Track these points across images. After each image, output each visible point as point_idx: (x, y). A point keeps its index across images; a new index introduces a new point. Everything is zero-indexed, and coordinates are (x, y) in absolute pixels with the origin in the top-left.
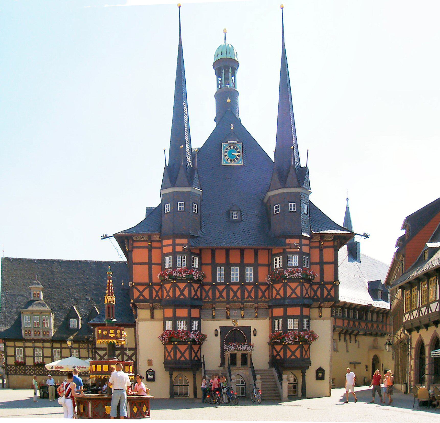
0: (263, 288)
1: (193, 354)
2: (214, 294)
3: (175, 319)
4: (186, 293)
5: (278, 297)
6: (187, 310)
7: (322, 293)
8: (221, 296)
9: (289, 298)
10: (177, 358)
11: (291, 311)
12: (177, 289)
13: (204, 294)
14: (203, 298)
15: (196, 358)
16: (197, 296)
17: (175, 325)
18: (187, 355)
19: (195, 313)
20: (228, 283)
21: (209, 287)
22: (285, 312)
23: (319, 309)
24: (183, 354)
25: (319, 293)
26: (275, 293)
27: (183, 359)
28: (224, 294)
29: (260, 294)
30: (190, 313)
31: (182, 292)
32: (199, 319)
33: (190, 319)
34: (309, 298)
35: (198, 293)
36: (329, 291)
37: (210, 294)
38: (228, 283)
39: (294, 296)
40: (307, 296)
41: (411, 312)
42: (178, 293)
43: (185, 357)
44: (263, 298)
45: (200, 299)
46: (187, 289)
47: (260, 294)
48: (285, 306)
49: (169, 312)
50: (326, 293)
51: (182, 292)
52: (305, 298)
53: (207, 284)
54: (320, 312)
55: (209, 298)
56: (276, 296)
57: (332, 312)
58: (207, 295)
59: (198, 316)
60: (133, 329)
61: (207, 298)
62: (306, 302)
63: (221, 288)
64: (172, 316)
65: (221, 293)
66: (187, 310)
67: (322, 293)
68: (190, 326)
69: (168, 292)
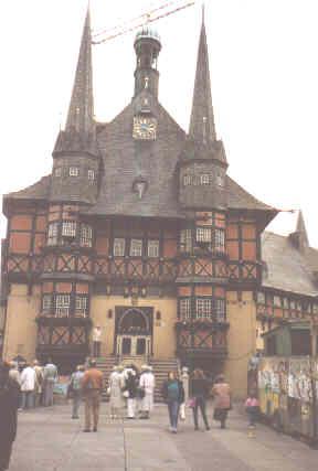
4: (71, 265)
7: (241, 272)
9: (197, 275)
10: (53, 343)
13: (97, 269)
19: (81, 289)
20: (127, 259)
25: (237, 273)
30: (74, 288)
32: (88, 297)
35: (88, 267)
38: (127, 259)
47: (165, 272)
54: (240, 295)
63: (118, 262)
67: (241, 274)
68: (73, 303)
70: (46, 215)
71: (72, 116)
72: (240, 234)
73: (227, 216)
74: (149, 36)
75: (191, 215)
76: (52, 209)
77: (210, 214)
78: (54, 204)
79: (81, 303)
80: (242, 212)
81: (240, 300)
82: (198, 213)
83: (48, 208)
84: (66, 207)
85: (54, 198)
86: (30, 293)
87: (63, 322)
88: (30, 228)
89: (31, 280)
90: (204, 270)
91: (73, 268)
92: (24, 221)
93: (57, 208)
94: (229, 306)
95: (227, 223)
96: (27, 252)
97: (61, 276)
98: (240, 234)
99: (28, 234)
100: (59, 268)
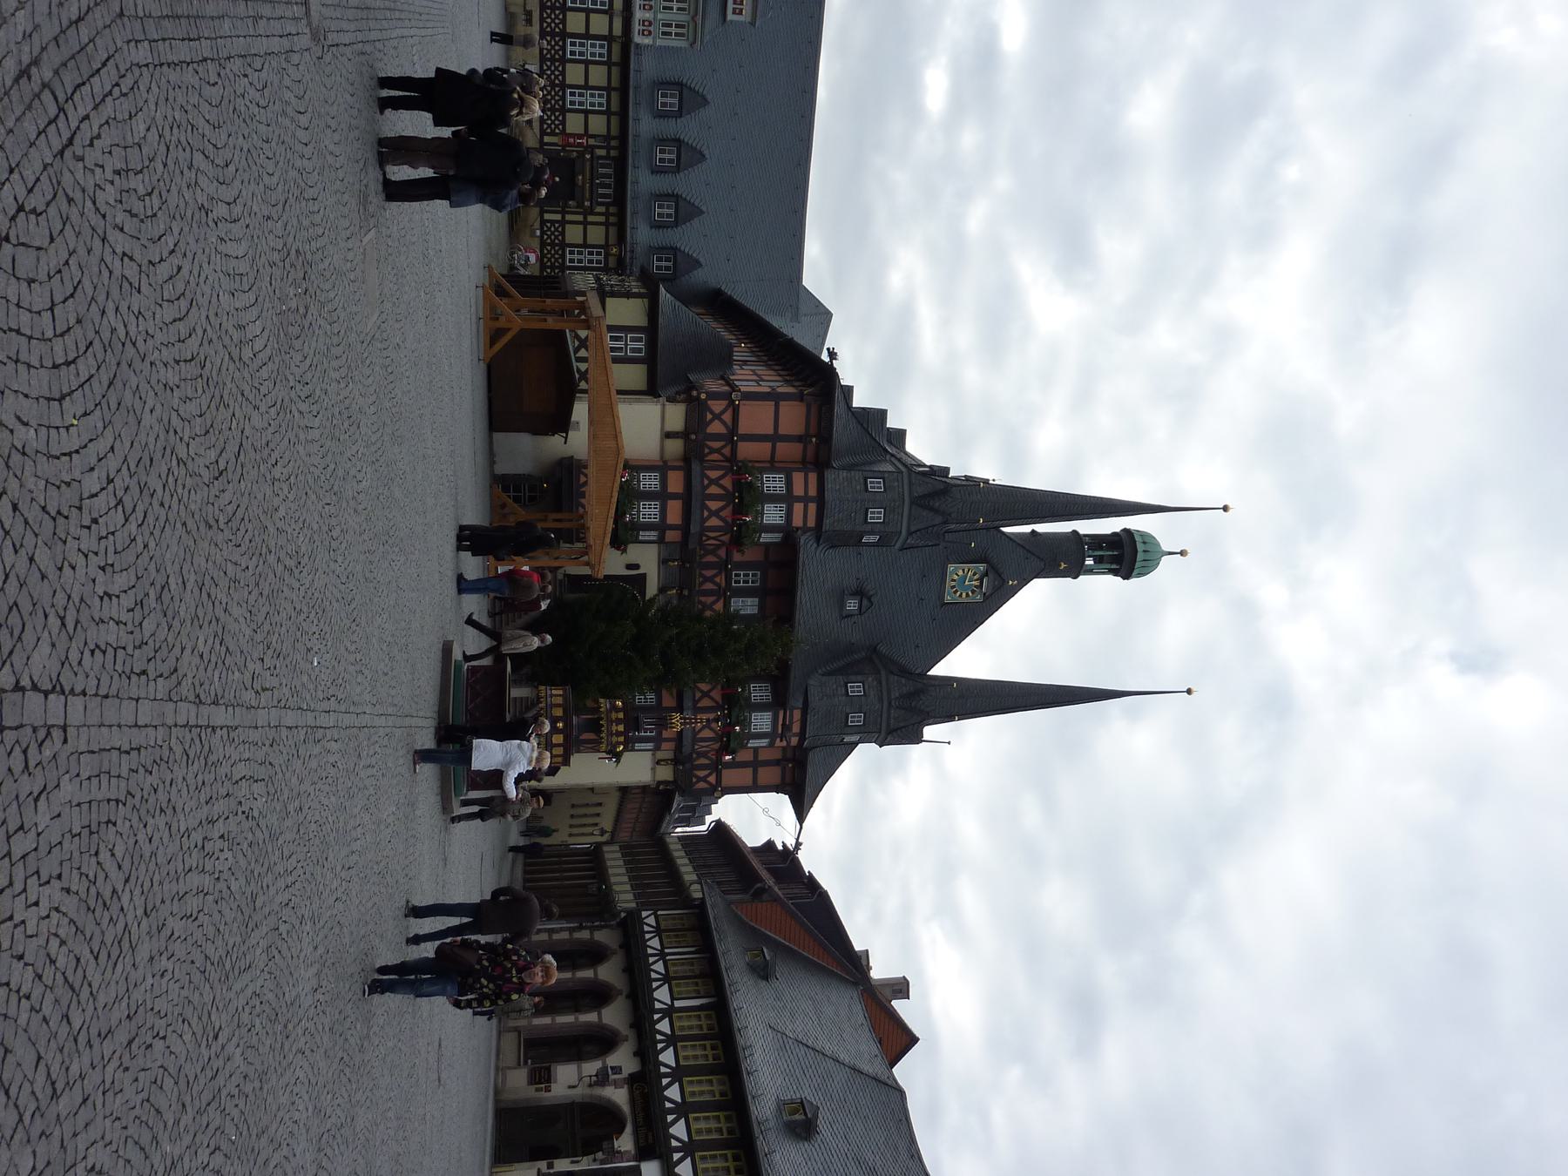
2: (709, 566)
3: (662, 496)
4: (714, 522)
5: (698, 695)
8: (707, 579)
12: (721, 504)
17: (649, 496)
28: (709, 586)
30: (672, 527)
31: (716, 513)
32: (661, 541)
33: (661, 527)
36: (704, 779)
37: (711, 558)
41: (658, 931)
45: (700, 542)
49: (676, 483)
50: (702, 773)
51: (716, 513)
55: (702, 557)
57: (666, 783)
58: (708, 553)
63: (721, 580)
65: (711, 579)
68: (649, 527)
72: (767, 763)
76: (813, 477)
77: (796, 728)
79: (652, 535)
81: (658, 763)
82: (797, 714)
85: (829, 475)
86: (668, 435)
88: (781, 431)
89: (692, 435)
96: (743, 429)
97: (695, 504)
98: (767, 763)
99: (771, 432)
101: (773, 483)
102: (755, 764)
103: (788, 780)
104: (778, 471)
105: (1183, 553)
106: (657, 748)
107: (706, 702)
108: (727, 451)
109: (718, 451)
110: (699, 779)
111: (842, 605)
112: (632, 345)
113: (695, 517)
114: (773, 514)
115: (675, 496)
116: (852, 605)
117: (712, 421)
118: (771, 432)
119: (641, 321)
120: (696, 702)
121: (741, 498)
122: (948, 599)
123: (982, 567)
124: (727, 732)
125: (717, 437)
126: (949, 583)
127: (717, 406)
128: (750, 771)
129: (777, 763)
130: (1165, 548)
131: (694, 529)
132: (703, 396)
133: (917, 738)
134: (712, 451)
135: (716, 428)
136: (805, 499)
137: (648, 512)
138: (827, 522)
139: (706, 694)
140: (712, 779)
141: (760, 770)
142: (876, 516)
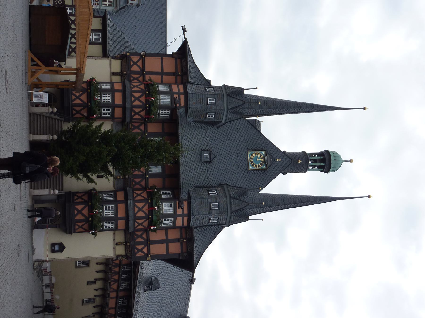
0: (143, 183)
1: (78, 109)
3: (112, 91)
4: (137, 103)
5: (135, 195)
6: (121, 103)
7: (140, 243)
9: (134, 205)
11: (121, 207)
13: (136, 125)
14: (133, 123)
15: (74, 112)
16: (134, 115)
18: (78, 102)
19: (118, 112)
21: (143, 130)
22: (121, 202)
23: (124, 243)
24: (78, 98)
25: (140, 240)
26: (139, 192)
27: (74, 97)
29: (137, 180)
30: (118, 106)
31: (138, 99)
33: (112, 106)
34: (135, 227)
35: (137, 117)
36: (141, 250)
39: (136, 210)
40: (136, 225)
42: (137, 95)
43: (75, 99)
44: (134, 183)
46: (140, 104)
47: (137, 180)
48: (126, 201)
49: (118, 87)
50: (140, 247)
51: (138, 99)
52: (135, 222)
53: (145, 128)
55: (132, 130)
56: (136, 193)
57: (121, 256)
58: (135, 127)
59: (115, 116)
60: (102, 56)
61: (133, 127)
62: (131, 223)
64: (115, 88)
66: (121, 103)
67: (140, 243)
69: (137, 86)
70: (176, 83)
71: (256, 100)
72: (173, 241)
73: (185, 227)
74: (333, 162)
75: (184, 195)
76: (181, 87)
77: (186, 212)
78: (185, 88)
80: (190, 240)
81: (117, 244)
83: (182, 83)
84: (182, 97)
85: (189, 86)
86: (114, 74)
87: (90, 97)
90: (140, 209)
91: (134, 104)
92: (170, 66)
93: (182, 90)
94: (112, 232)
95: (181, 228)
98: (173, 241)
99: (160, 71)
100: (134, 94)
101: (163, 88)
102: (167, 241)
103: (184, 250)
104: (165, 84)
105: (351, 161)
106: (116, 229)
107: (139, 198)
108: (141, 79)
109: (137, 79)
110: (139, 251)
111: (201, 156)
112: (95, 37)
113: (128, 100)
114: (165, 100)
115: (118, 91)
116: (206, 156)
117: (133, 65)
118: (160, 71)
119: (99, 27)
120: (134, 198)
121: (149, 91)
122: (250, 168)
123: (264, 152)
124: (151, 211)
125: (135, 72)
126: (250, 160)
127: (135, 59)
128: (164, 246)
129: (178, 240)
130: (344, 159)
131: (128, 105)
132: (128, 54)
133: (247, 219)
134: (134, 79)
135: (135, 68)
136: (179, 93)
137: (106, 98)
138: (190, 103)
139: (138, 195)
140: (145, 250)
141: (170, 245)
142: (212, 101)
